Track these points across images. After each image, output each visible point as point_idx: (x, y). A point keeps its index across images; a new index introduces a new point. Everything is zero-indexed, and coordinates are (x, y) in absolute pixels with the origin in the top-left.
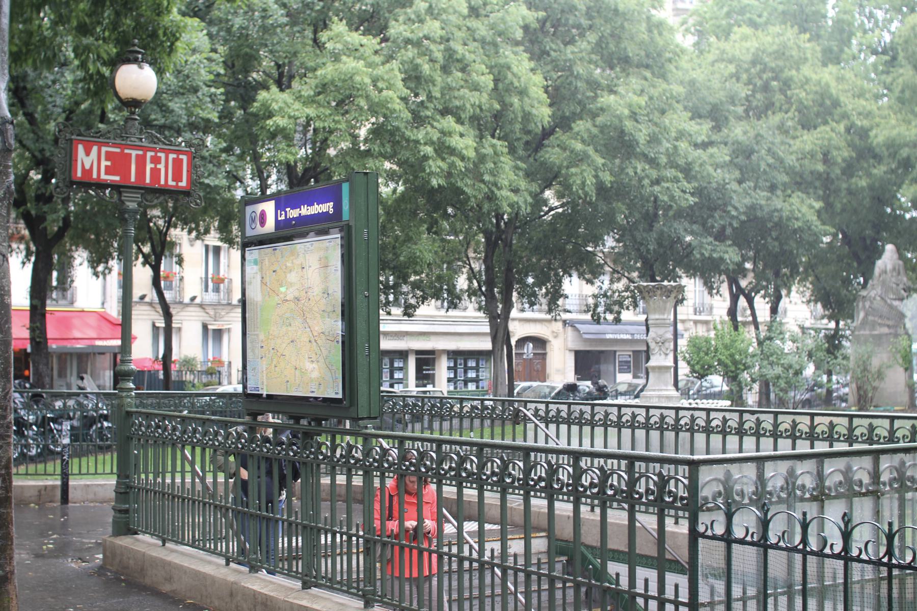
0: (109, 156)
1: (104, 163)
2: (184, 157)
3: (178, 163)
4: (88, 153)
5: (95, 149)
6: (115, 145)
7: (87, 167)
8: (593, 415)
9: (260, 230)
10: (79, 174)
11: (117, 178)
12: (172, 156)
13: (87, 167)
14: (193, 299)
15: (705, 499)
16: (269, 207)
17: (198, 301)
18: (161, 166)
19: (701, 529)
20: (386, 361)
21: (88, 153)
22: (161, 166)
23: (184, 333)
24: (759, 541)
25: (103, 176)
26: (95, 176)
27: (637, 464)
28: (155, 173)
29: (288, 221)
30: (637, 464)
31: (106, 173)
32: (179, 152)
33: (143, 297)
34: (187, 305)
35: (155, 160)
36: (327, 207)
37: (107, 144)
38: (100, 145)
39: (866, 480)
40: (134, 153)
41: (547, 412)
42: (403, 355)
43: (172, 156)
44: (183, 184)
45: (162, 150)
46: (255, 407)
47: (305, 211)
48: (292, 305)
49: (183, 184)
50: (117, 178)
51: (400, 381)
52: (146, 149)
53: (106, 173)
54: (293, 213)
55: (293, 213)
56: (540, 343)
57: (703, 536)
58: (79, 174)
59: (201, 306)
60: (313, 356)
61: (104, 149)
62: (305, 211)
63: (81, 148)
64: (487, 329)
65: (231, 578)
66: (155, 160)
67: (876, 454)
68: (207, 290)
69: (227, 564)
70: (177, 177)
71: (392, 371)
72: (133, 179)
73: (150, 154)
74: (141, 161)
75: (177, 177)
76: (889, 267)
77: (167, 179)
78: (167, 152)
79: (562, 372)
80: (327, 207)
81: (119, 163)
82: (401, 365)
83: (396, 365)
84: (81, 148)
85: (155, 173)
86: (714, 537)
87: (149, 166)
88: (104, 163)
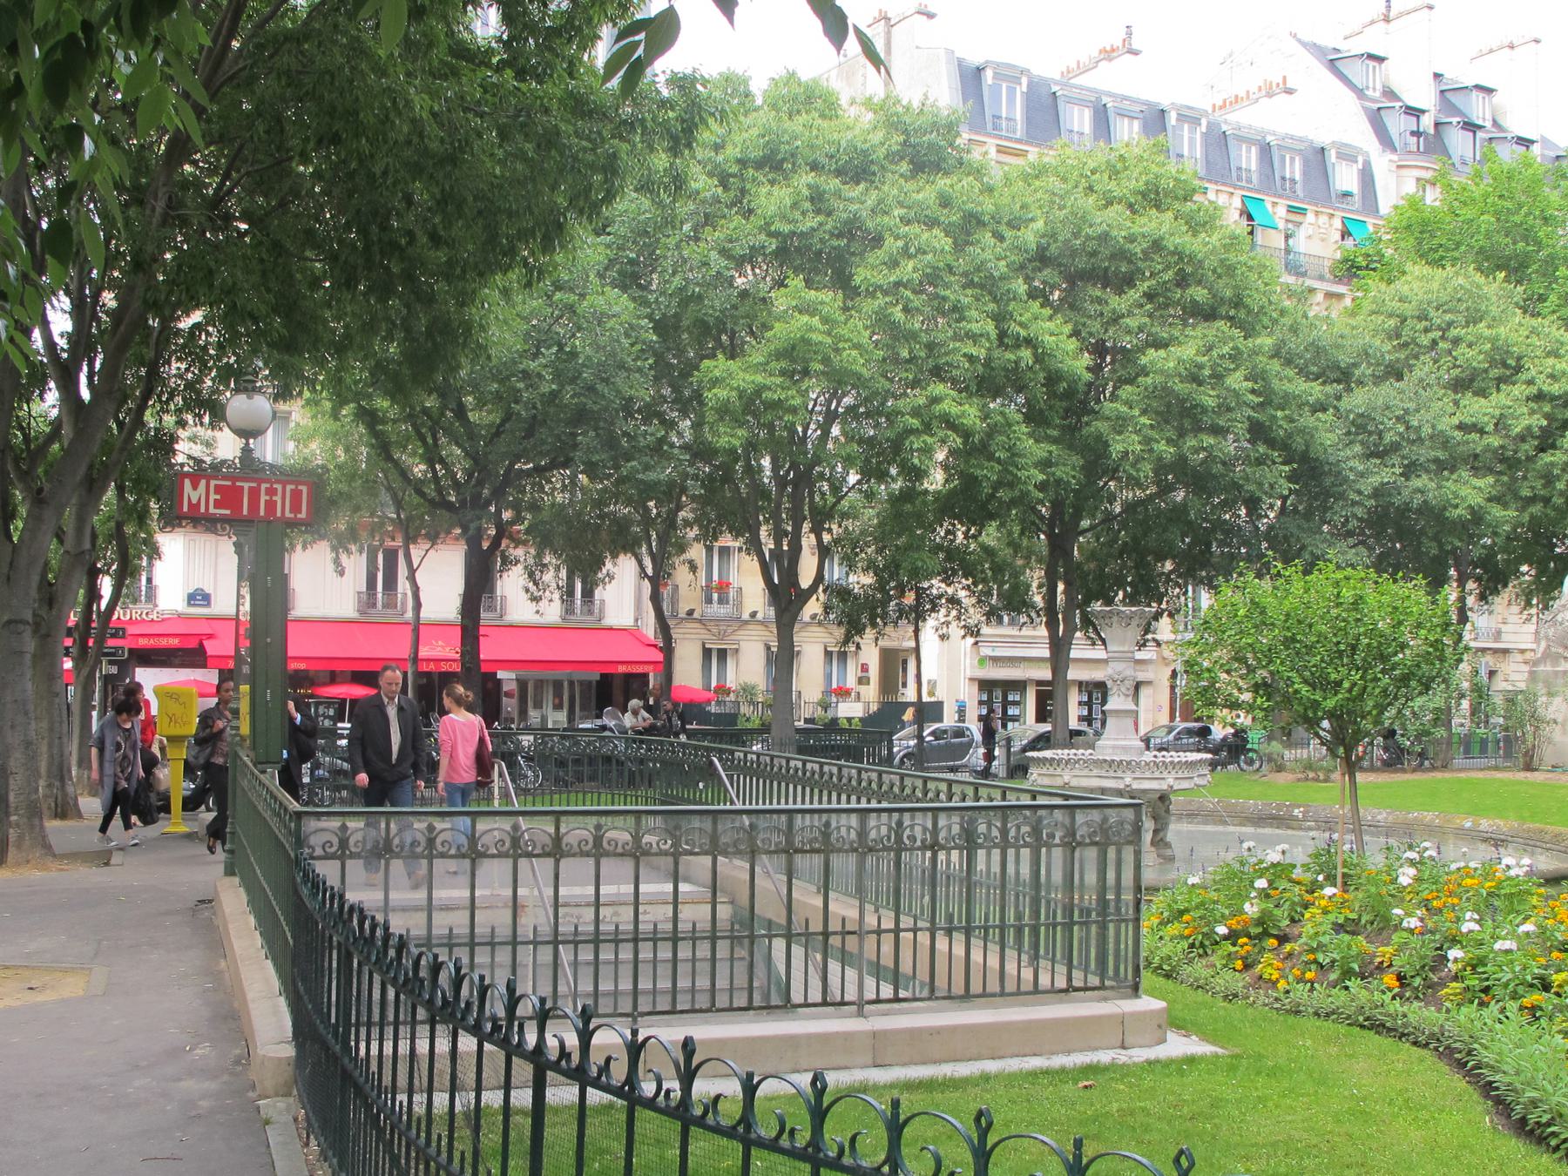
2: (304, 489)
7: (194, 501)
10: (185, 509)
12: (289, 488)
13: (194, 501)
14: (753, 615)
17: (760, 616)
18: (278, 498)
20: (998, 693)
22: (278, 498)
23: (743, 656)
24: (805, 1148)
26: (203, 510)
31: (216, 507)
33: (691, 612)
34: (746, 622)
42: (1020, 686)
51: (1015, 719)
53: (216, 507)
58: (185, 509)
59: (762, 623)
71: (1006, 704)
72: (245, 512)
73: (264, 486)
74: (254, 494)
82: (1017, 698)
83: (1010, 698)
85: (271, 506)
87: (264, 498)
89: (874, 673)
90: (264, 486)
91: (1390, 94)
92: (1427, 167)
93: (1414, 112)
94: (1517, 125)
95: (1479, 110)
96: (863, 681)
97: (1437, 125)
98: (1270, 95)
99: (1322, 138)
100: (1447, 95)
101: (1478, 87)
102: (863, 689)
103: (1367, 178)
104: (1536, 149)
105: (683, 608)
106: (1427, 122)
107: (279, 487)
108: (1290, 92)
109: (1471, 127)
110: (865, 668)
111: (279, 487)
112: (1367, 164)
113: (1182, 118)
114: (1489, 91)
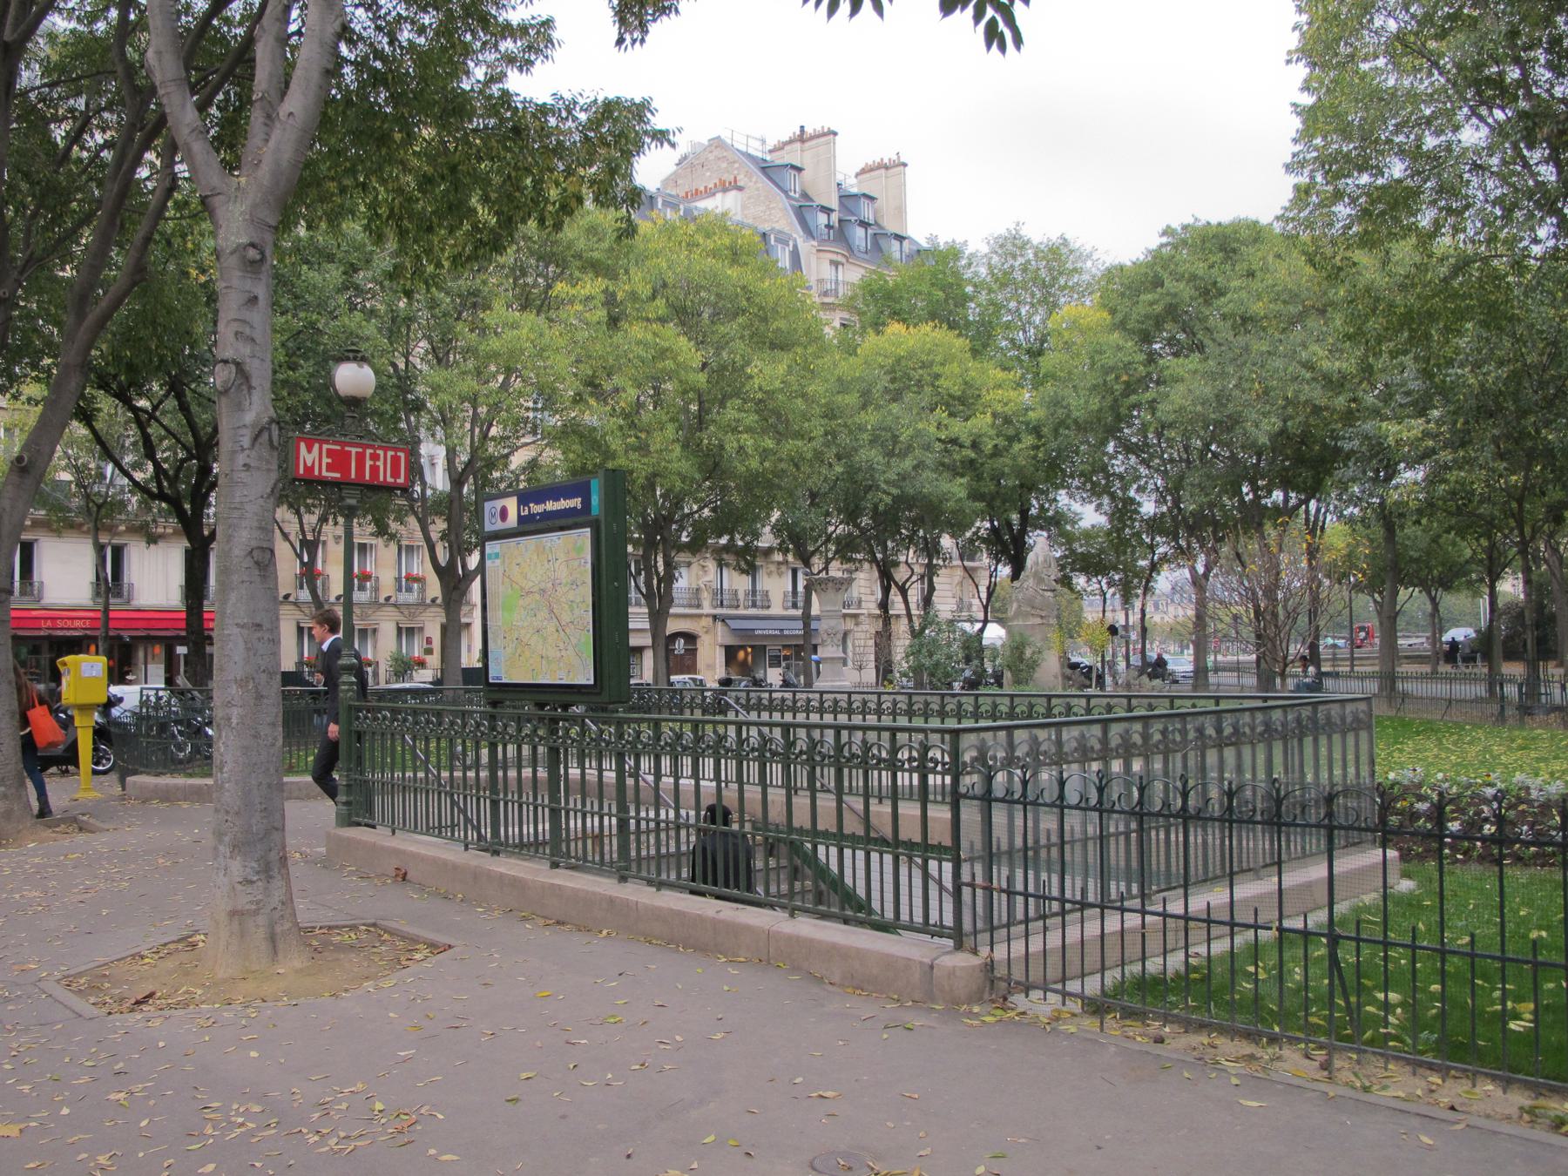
0: (330, 453)
1: (325, 460)
3: (396, 460)
4: (309, 450)
5: (317, 446)
6: (335, 443)
8: (795, 702)
9: (500, 526)
11: (337, 475)
12: (390, 453)
15: (965, 764)
16: (511, 504)
18: (380, 463)
19: (963, 790)
21: (309, 450)
25: (325, 473)
27: (899, 735)
28: (375, 469)
29: (531, 516)
30: (899, 735)
32: (396, 450)
35: (375, 457)
36: (576, 503)
37: (327, 442)
38: (321, 442)
39: (1097, 747)
40: (354, 450)
41: (748, 700)
43: (390, 453)
44: (401, 480)
45: (380, 448)
46: (497, 696)
47: (551, 506)
48: (537, 597)
49: (401, 480)
50: (337, 475)
52: (366, 447)
54: (537, 509)
55: (537, 509)
56: (690, 638)
57: (965, 796)
60: (562, 646)
61: (325, 447)
62: (551, 506)
63: (303, 446)
64: (647, 626)
65: (474, 863)
66: (375, 457)
67: (1105, 723)
68: (400, 590)
69: (466, 848)
70: (396, 474)
73: (369, 451)
74: (361, 458)
75: (396, 474)
76: (1041, 559)
77: (385, 476)
78: (386, 450)
79: (711, 667)
80: (576, 503)
81: (339, 461)
84: (303, 446)
85: (375, 469)
86: (974, 798)
87: (368, 463)
88: (325, 460)
89: (436, 645)
90: (369, 451)
91: (805, 196)
92: (837, 251)
93: (827, 210)
94: (891, 227)
95: (867, 212)
96: (429, 652)
97: (840, 221)
98: (725, 190)
99: (766, 227)
100: (847, 199)
101: (865, 196)
102: (428, 658)
103: (795, 256)
104: (906, 243)
105: (282, 593)
106: (835, 217)
107: (381, 453)
108: (740, 189)
109: (864, 224)
110: (429, 641)
111: (381, 453)
112: (795, 246)
113: (666, 204)
114: (872, 199)
